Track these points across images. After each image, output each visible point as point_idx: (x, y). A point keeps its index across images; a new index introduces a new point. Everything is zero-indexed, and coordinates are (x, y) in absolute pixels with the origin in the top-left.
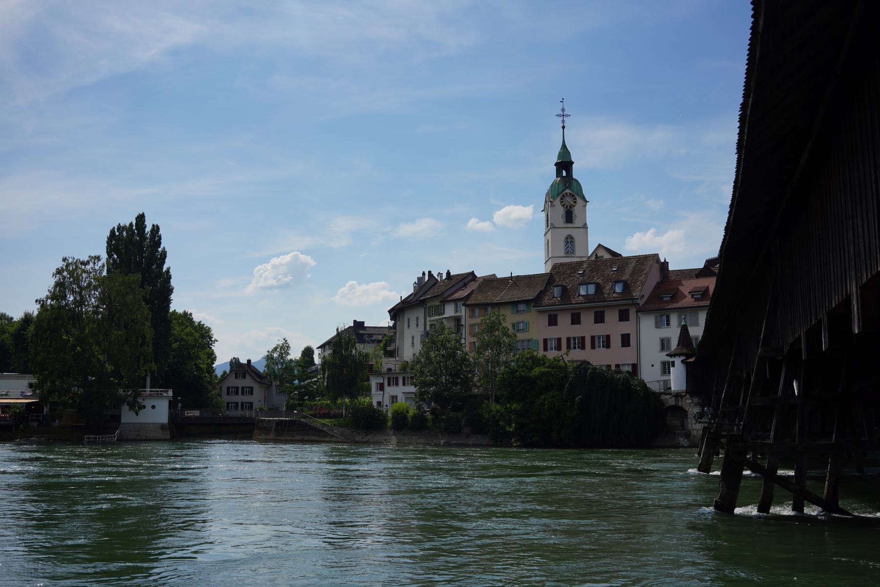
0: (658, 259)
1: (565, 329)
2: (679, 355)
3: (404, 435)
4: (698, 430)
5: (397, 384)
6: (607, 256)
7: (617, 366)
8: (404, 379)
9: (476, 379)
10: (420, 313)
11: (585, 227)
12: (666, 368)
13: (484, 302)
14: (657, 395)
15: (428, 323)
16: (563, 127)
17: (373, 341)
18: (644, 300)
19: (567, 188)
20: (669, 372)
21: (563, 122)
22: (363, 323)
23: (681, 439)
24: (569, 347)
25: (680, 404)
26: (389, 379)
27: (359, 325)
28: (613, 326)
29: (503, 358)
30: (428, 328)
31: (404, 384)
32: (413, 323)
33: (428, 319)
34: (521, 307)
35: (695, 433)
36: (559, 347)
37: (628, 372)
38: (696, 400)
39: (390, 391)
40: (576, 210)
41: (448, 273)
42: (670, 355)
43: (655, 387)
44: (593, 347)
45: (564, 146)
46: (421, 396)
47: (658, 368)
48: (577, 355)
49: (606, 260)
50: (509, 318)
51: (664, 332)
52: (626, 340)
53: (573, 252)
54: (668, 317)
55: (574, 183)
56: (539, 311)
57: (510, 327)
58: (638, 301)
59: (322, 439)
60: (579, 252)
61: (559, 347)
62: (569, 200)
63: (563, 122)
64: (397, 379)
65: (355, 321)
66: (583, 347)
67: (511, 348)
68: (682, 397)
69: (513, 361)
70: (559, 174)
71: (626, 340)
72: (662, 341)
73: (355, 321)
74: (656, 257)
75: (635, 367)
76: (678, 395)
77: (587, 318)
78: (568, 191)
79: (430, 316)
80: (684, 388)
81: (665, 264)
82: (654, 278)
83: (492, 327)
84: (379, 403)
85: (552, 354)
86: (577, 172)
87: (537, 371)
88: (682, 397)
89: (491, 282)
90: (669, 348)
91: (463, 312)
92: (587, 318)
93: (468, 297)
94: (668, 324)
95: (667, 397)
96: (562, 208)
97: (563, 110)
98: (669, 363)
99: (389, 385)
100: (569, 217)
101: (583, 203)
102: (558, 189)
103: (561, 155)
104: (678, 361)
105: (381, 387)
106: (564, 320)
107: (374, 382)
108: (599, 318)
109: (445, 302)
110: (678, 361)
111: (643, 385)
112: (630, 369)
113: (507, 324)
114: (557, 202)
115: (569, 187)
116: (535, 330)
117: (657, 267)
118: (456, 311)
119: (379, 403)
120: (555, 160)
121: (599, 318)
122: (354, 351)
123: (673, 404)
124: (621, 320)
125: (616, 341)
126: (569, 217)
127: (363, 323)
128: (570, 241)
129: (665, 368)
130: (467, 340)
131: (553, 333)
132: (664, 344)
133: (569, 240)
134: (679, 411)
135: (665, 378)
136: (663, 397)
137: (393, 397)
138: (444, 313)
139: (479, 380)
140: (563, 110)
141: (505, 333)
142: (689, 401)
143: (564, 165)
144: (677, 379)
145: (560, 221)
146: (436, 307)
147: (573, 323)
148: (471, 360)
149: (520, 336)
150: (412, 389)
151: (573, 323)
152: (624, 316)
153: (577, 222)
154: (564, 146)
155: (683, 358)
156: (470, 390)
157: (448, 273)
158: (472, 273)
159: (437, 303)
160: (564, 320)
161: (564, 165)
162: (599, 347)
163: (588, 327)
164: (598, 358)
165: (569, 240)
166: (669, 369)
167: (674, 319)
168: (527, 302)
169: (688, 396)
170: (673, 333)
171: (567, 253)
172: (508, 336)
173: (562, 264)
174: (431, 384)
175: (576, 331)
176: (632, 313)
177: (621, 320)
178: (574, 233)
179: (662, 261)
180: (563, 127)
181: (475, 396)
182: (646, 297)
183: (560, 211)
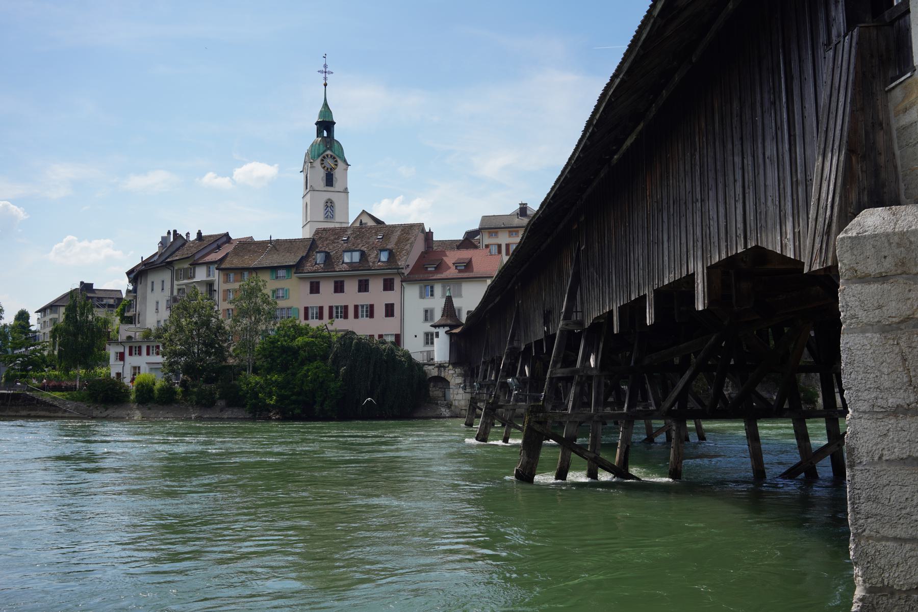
0: (423, 230)
1: (327, 297)
2: (444, 326)
3: (149, 409)
4: (459, 400)
5: (140, 354)
6: (371, 223)
7: (381, 336)
8: (148, 348)
9: (231, 349)
10: (166, 276)
11: (346, 191)
12: (429, 339)
13: (240, 266)
14: (420, 366)
15: (176, 287)
16: (325, 85)
17: (104, 306)
18: (409, 270)
19: (328, 149)
20: (432, 343)
21: (325, 78)
22: (92, 285)
23: (443, 410)
24: (331, 317)
25: (443, 375)
26: (131, 348)
27: (86, 287)
28: (377, 296)
29: (262, 327)
30: (175, 293)
31: (148, 354)
32: (158, 287)
33: (176, 283)
34: (281, 273)
36: (320, 317)
37: (392, 342)
38: (458, 370)
39: (132, 361)
40: (337, 174)
41: (199, 234)
42: (435, 326)
43: (418, 358)
44: (356, 316)
45: (326, 105)
46: (171, 367)
47: (421, 338)
48: (341, 325)
49: (371, 227)
50: (269, 284)
51: (428, 303)
52: (390, 310)
53: (333, 217)
54: (432, 287)
55: (336, 144)
56: (300, 278)
57: (270, 294)
58: (403, 271)
59: (52, 415)
60: (338, 218)
61: (320, 317)
62: (330, 162)
63: (325, 78)
64: (140, 347)
65: (82, 283)
66: (346, 317)
67: (271, 316)
68: (445, 367)
69: (272, 330)
70: (319, 133)
71: (390, 310)
72: (426, 311)
73: (82, 283)
74: (421, 226)
75: (398, 337)
76: (441, 366)
77: (351, 286)
78: (329, 152)
79: (177, 280)
80: (447, 359)
81: (429, 235)
82: (419, 248)
83: (251, 293)
84: (119, 374)
85: (314, 324)
86: (338, 134)
87: (300, 340)
88: (445, 367)
89: (247, 245)
90: (432, 319)
91: (216, 276)
92: (351, 286)
93: (222, 260)
94: (432, 295)
95: (430, 368)
96: (322, 170)
97: (325, 66)
98: (432, 335)
99: (131, 354)
100: (329, 180)
101: (345, 166)
102: (319, 149)
103: (322, 114)
104: (442, 331)
105: (121, 357)
106: (327, 288)
107: (112, 351)
108: (363, 287)
109: (195, 264)
110: (442, 331)
111: (408, 355)
112: (393, 339)
113: (267, 291)
114: (317, 163)
115: (330, 149)
116: (295, 296)
117: (421, 237)
118: (209, 275)
119: (119, 374)
120: (316, 119)
121: (363, 287)
122: (90, 317)
123: (436, 374)
124: (385, 289)
125: (380, 311)
126: (329, 180)
127: (92, 285)
128: (329, 205)
129: (427, 339)
130: (223, 306)
131: (315, 301)
132: (428, 314)
133: (329, 204)
134: (442, 382)
135: (428, 348)
136: (426, 368)
137: (135, 368)
138: (194, 277)
139: (234, 351)
140: (325, 66)
141: (265, 301)
143: (326, 125)
144: (441, 350)
145: (320, 182)
146: (186, 270)
147: (336, 291)
148: (227, 328)
149: (281, 303)
150: (159, 359)
151: (336, 291)
152: (388, 286)
153: (338, 186)
154: (326, 105)
155: (447, 329)
156: (225, 360)
157: (199, 234)
158: (227, 235)
159: (186, 266)
160: (327, 288)
161: (326, 125)
162: (362, 316)
163: (351, 296)
164: (363, 328)
165: (329, 204)
166: (432, 339)
167: (438, 289)
168: (288, 268)
169: (451, 367)
170: (437, 304)
171: (327, 217)
172: (268, 303)
173: (325, 230)
174: (182, 354)
175: (339, 300)
176: (397, 283)
177: (385, 289)
178: (334, 197)
179: (427, 230)
180: (325, 85)
181: (230, 367)
182: (411, 267)
183: (321, 173)
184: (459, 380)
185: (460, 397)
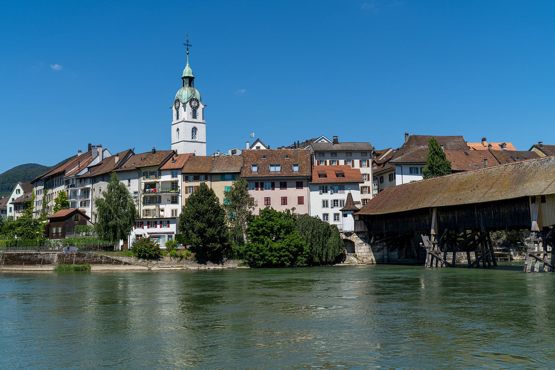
2: (350, 210)
21: (188, 49)
35: (360, 254)
52: (301, 201)
63: (188, 49)
71: (301, 201)
72: (324, 201)
76: (348, 234)
80: (353, 229)
97: (188, 41)
101: (203, 107)
118: (173, 177)
140: (188, 41)
142: (357, 236)
144: (348, 224)
169: (355, 234)
178: (197, 125)
184: (361, 241)
185: (362, 251)
